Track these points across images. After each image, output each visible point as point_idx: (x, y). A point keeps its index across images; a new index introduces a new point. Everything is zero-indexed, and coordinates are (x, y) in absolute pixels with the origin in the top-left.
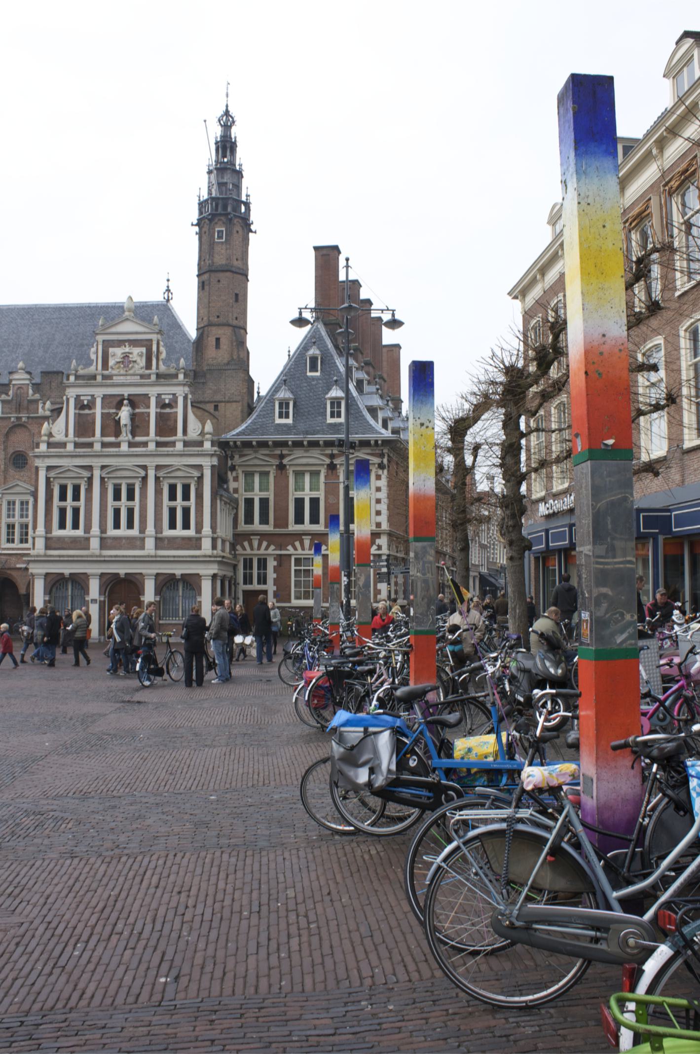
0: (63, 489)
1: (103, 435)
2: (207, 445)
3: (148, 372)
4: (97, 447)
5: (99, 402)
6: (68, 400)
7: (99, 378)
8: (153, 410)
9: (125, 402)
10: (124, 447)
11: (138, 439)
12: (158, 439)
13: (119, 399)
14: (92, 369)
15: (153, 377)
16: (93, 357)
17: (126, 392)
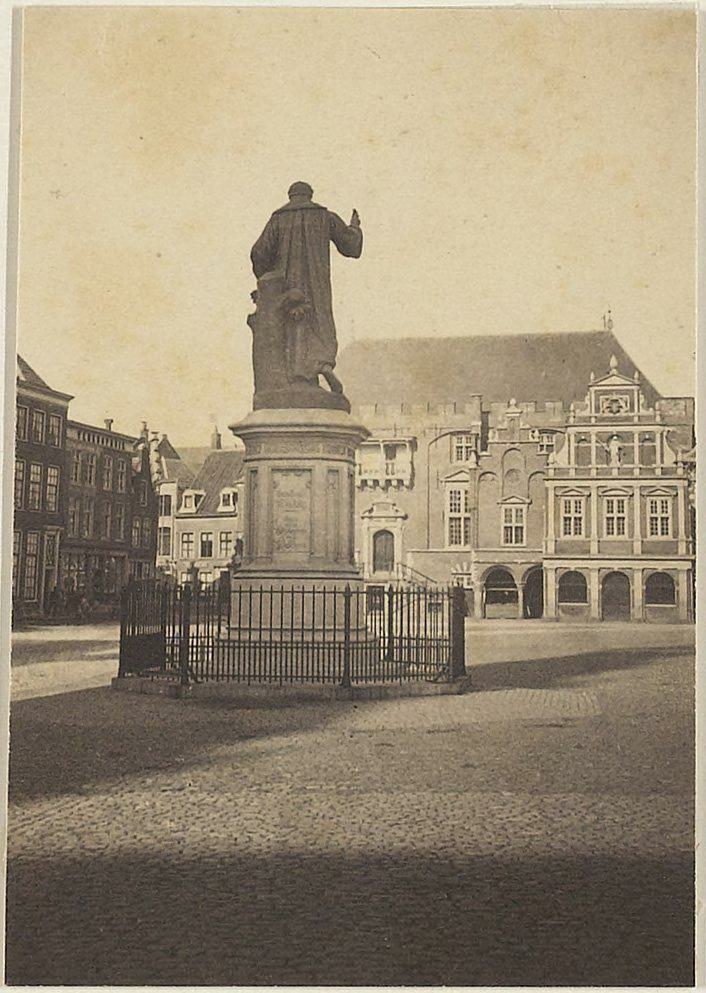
0: (567, 504)
1: (597, 463)
2: (680, 471)
3: (631, 414)
4: (594, 473)
5: (594, 438)
6: (569, 436)
7: (593, 420)
8: (636, 443)
9: (615, 438)
10: (615, 472)
11: (625, 466)
12: (641, 466)
13: (606, 436)
14: (586, 413)
15: (636, 419)
16: (587, 402)
17: (614, 430)
